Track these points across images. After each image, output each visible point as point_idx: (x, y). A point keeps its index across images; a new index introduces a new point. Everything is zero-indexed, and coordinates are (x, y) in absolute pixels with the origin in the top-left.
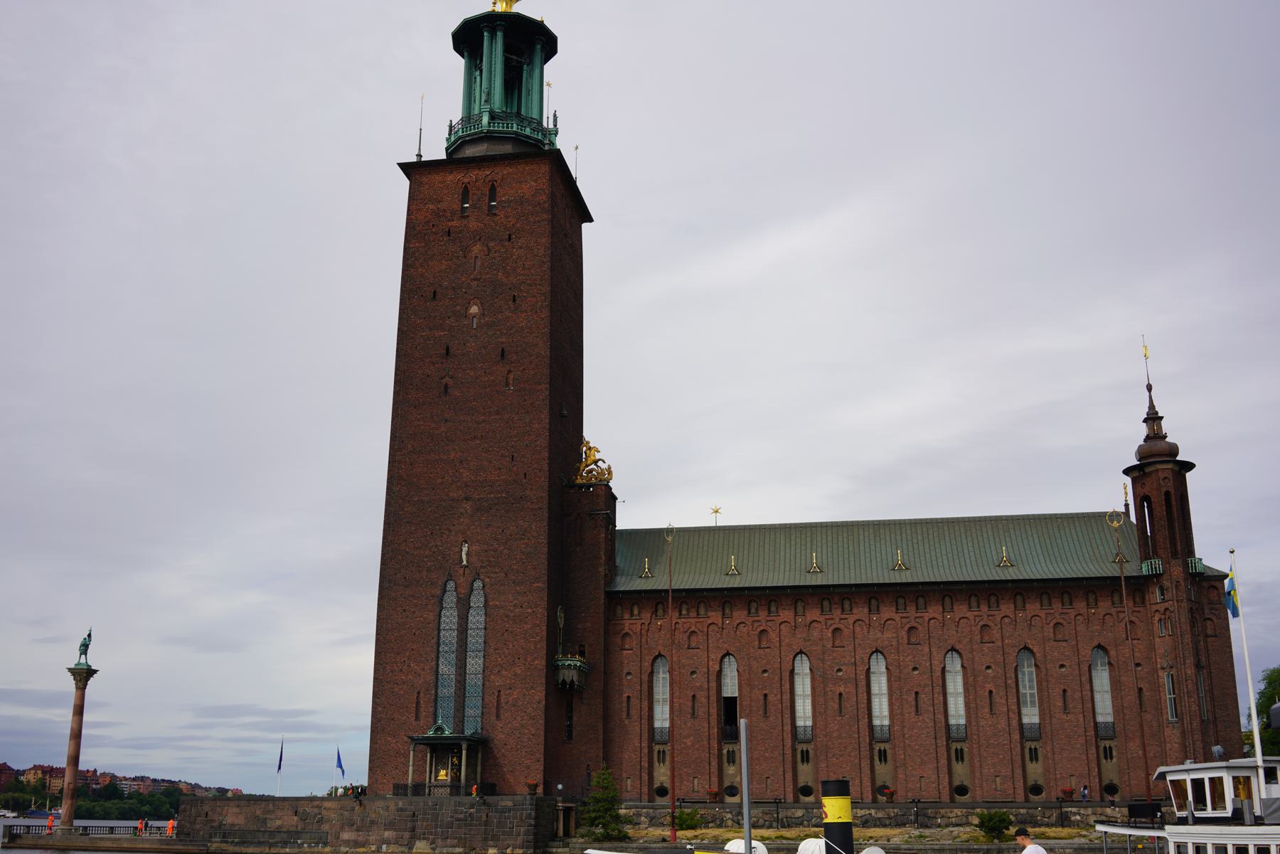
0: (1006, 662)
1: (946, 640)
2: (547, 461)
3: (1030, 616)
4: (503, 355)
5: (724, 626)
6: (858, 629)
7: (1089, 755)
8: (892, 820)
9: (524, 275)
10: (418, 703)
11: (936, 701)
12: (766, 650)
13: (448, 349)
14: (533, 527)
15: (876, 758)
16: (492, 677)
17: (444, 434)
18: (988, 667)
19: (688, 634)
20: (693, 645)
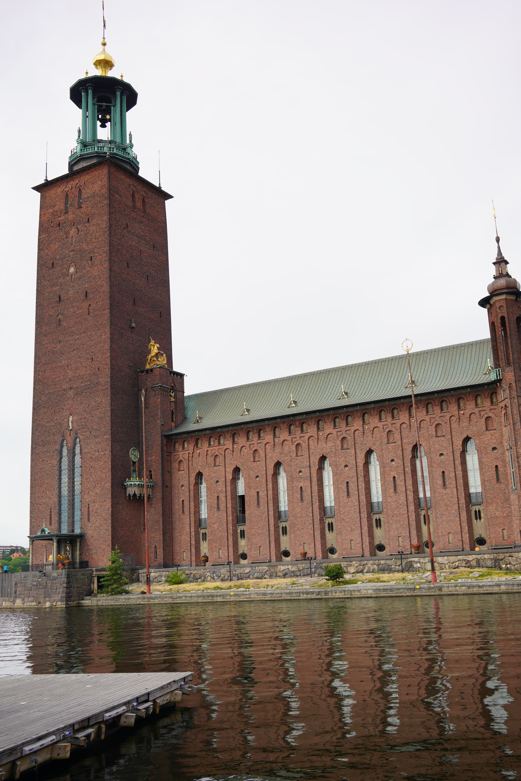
0: (404, 455)
1: (366, 444)
2: (109, 358)
4: (86, 296)
5: (234, 450)
6: (311, 443)
7: (462, 518)
8: (301, 572)
9: (95, 242)
10: (51, 515)
11: (360, 487)
14: (103, 401)
15: (327, 529)
17: (59, 351)
18: (392, 460)
19: (214, 457)
20: (217, 464)
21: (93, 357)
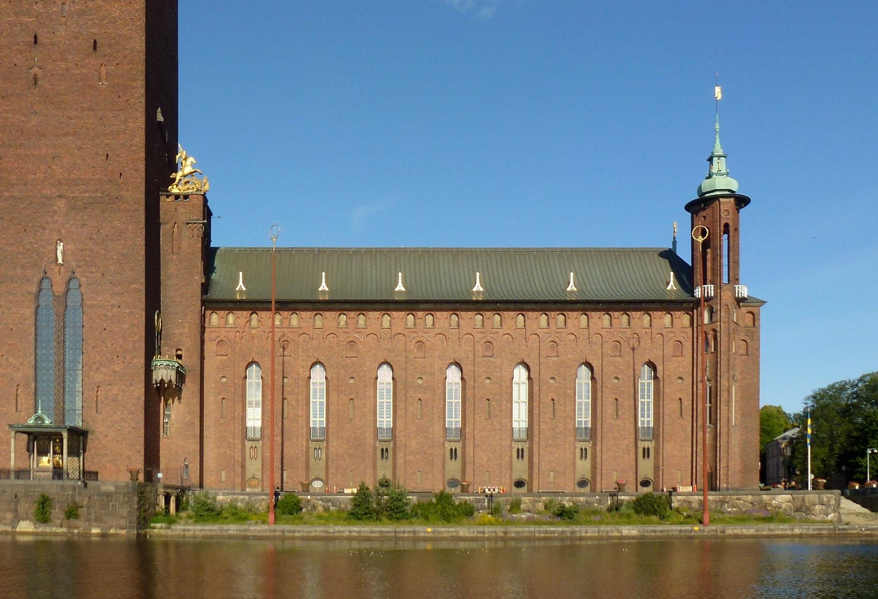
4: (95, 48)
13: (36, 37)
16: (91, 373)
21: (109, 153)
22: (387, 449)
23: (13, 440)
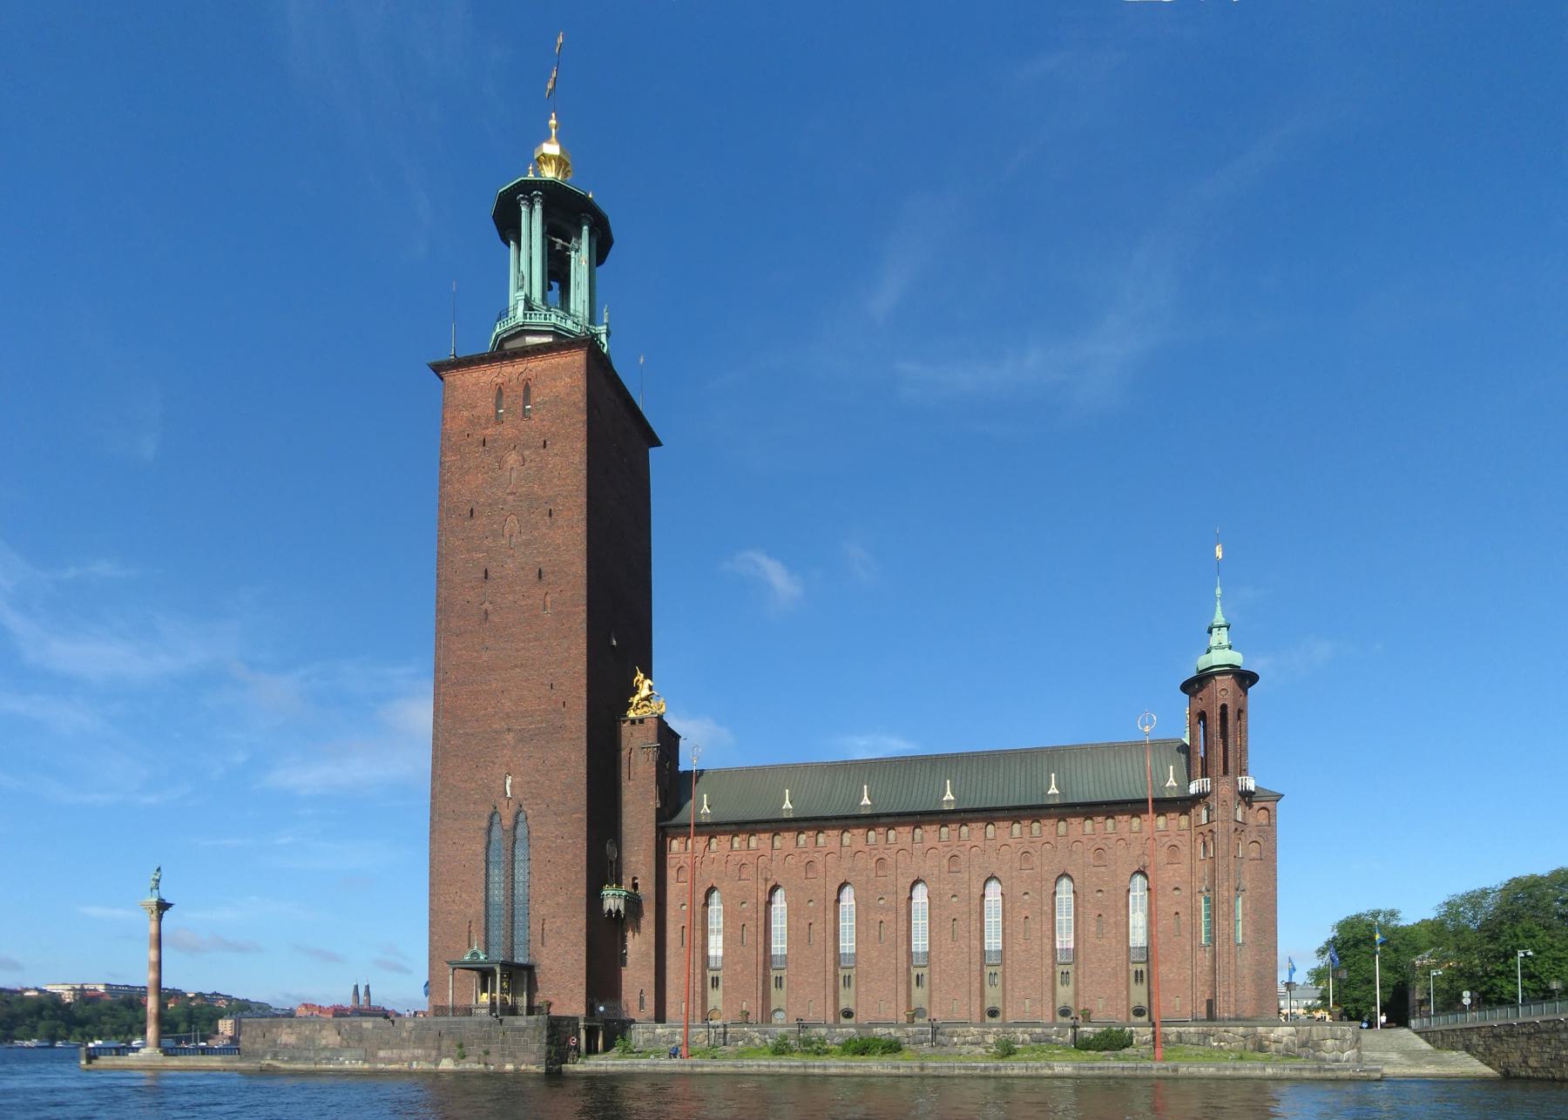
3: (1071, 842)
4: (540, 577)
6: (900, 858)
12: (813, 880)
14: (573, 757)
22: (849, 976)
23: (451, 977)
